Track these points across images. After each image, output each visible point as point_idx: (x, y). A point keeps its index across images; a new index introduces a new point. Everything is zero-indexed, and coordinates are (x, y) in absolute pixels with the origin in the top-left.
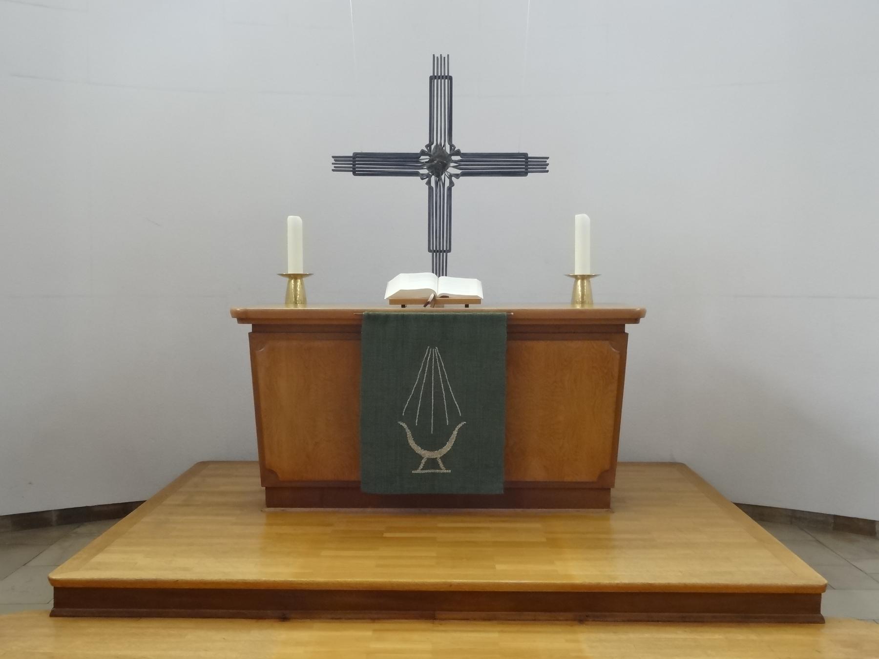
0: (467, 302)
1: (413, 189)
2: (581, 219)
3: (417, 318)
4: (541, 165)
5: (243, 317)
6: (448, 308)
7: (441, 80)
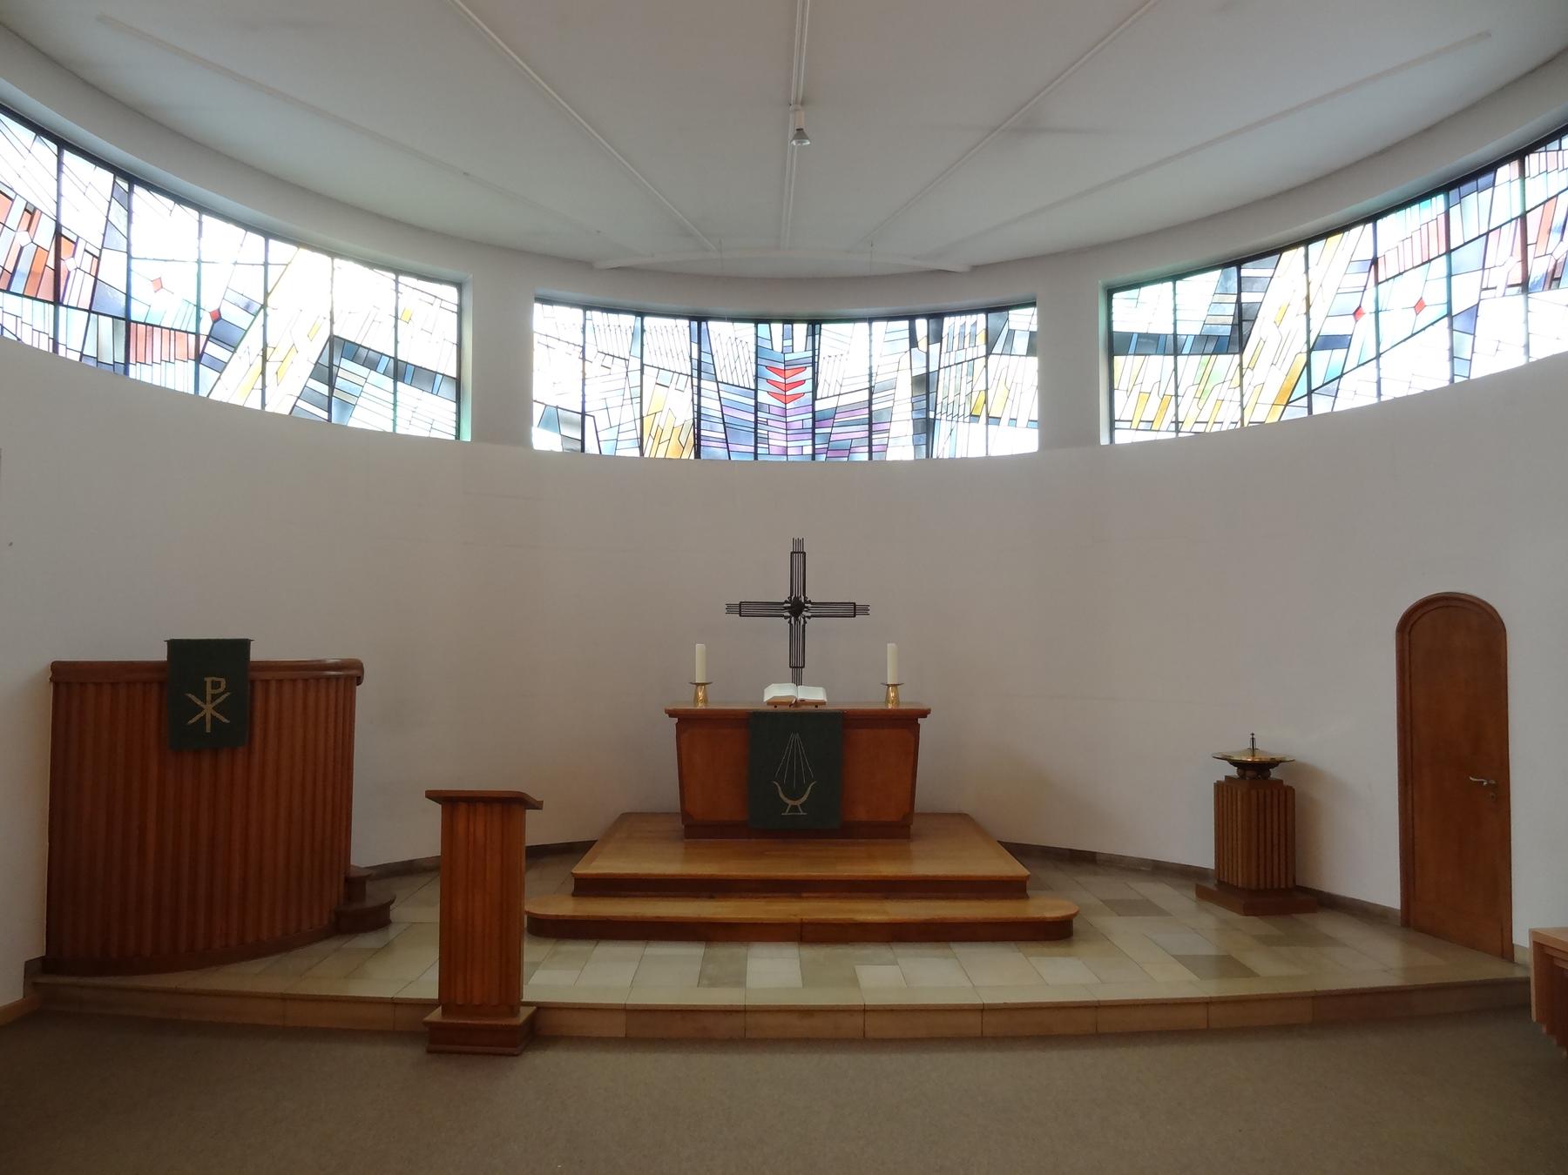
0: (817, 704)
2: (891, 647)
3: (785, 714)
4: (865, 610)
5: (672, 714)
6: (803, 708)
7: (798, 554)
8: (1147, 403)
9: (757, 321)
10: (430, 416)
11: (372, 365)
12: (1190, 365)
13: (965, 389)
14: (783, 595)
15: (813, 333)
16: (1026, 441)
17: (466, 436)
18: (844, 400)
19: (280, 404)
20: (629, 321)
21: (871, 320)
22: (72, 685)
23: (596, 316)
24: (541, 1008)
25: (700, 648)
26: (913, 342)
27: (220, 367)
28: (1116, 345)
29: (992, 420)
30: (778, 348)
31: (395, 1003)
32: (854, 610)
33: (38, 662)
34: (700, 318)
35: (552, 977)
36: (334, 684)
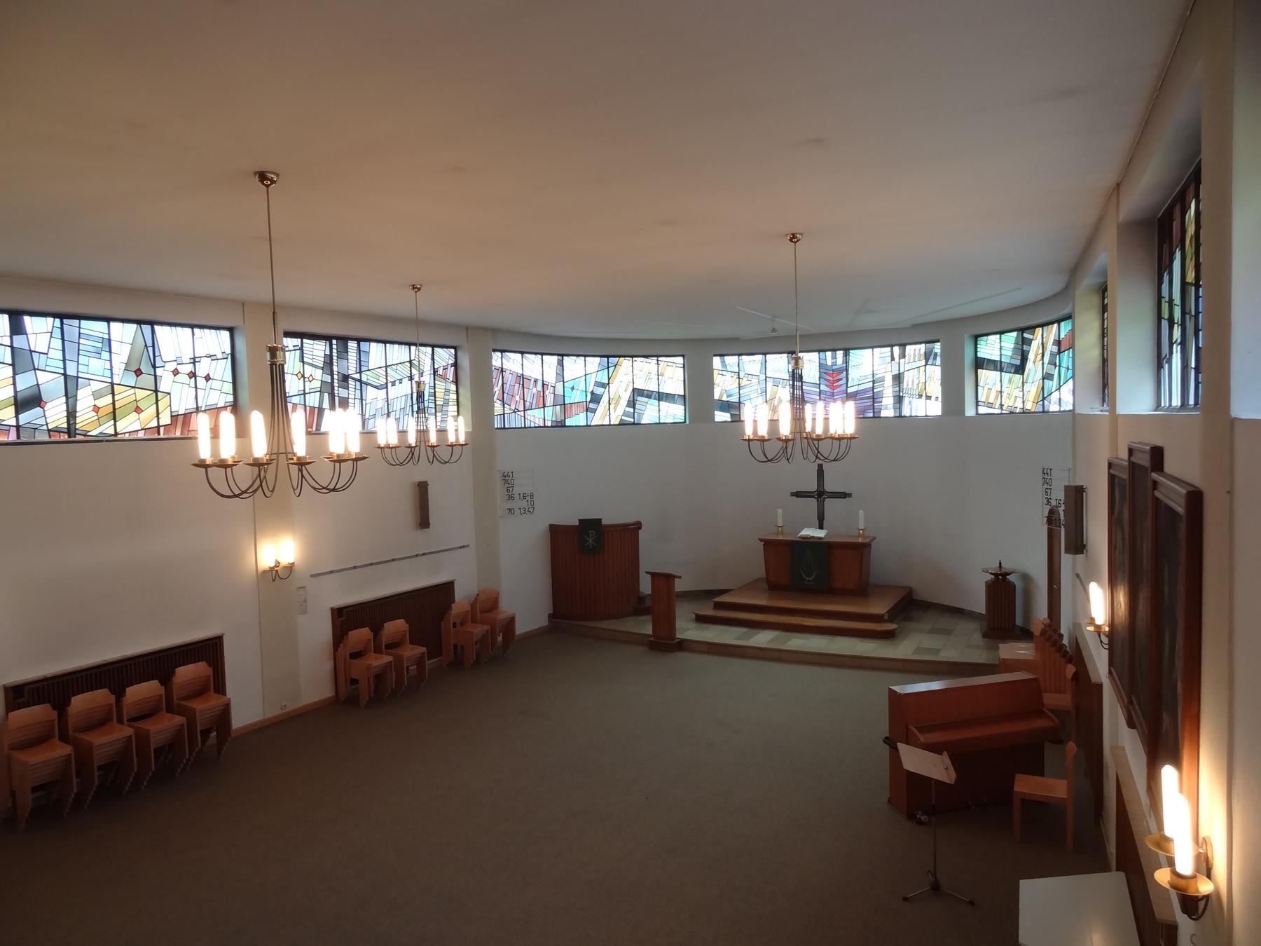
1: (813, 502)
4: (849, 495)
8: (997, 393)
9: (819, 351)
10: (674, 413)
11: (649, 396)
13: (916, 382)
15: (846, 355)
20: (760, 357)
21: (873, 348)
23: (744, 358)
24: (683, 640)
26: (893, 359)
27: (594, 411)
28: (980, 363)
29: (928, 398)
30: (829, 363)
32: (844, 495)
36: (631, 531)
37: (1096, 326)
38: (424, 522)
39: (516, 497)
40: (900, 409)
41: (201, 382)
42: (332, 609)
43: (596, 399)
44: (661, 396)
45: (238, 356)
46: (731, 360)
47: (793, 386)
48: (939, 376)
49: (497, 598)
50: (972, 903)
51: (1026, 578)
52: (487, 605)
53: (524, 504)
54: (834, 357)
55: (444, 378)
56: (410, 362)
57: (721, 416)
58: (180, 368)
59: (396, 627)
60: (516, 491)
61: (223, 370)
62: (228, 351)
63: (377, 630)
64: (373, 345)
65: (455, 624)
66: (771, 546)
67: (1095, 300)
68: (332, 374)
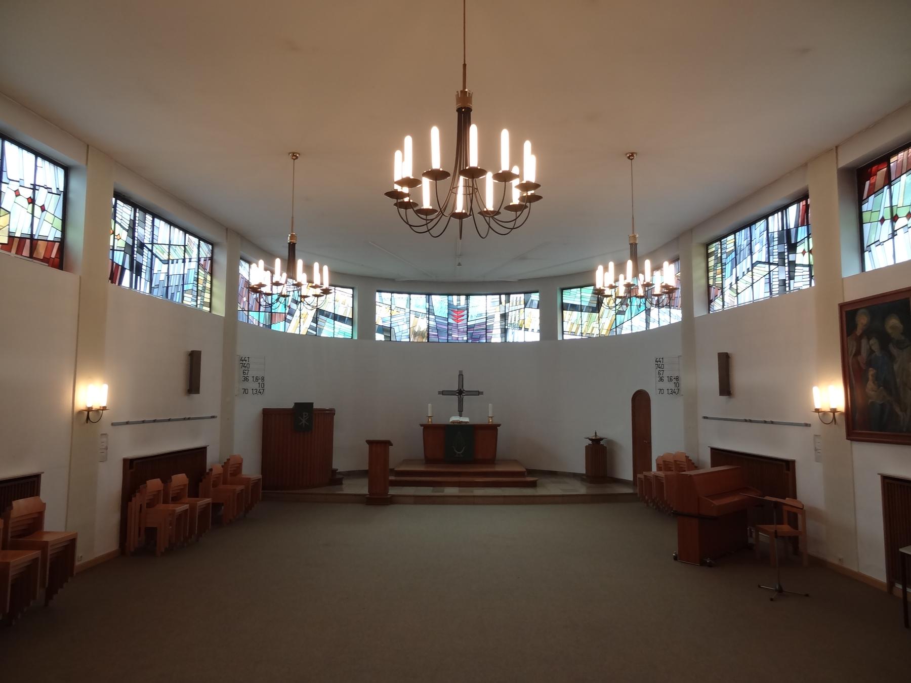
1: (456, 398)
4: (482, 393)
5: (421, 425)
7: (461, 375)
8: (573, 325)
9: (448, 295)
10: (344, 331)
11: (327, 316)
12: (585, 315)
14: (456, 388)
15: (467, 299)
16: (535, 337)
17: (355, 338)
18: (477, 322)
19: (303, 332)
20: (406, 296)
21: (486, 295)
22: (268, 414)
23: (395, 295)
24: (393, 496)
25: (430, 405)
26: (501, 303)
27: (290, 321)
28: (564, 307)
29: (526, 329)
31: (355, 495)
33: (260, 409)
34: (429, 294)
35: (393, 491)
37: (703, 265)
38: (193, 386)
39: (250, 379)
40: (506, 337)
41: (38, 210)
42: (125, 460)
43: (291, 313)
44: (336, 317)
45: (71, 195)
46: (386, 296)
47: (429, 318)
48: (538, 316)
49: (241, 464)
50: (807, 595)
51: (611, 442)
52: (233, 468)
53: (255, 385)
54: (458, 300)
55: (205, 269)
56: (185, 246)
57: (380, 337)
58: (22, 190)
59: (180, 479)
60: (251, 373)
61: (54, 204)
62: (62, 189)
63: (166, 480)
64: (162, 223)
65: (215, 485)
66: (429, 429)
67: (703, 250)
68: (133, 238)
